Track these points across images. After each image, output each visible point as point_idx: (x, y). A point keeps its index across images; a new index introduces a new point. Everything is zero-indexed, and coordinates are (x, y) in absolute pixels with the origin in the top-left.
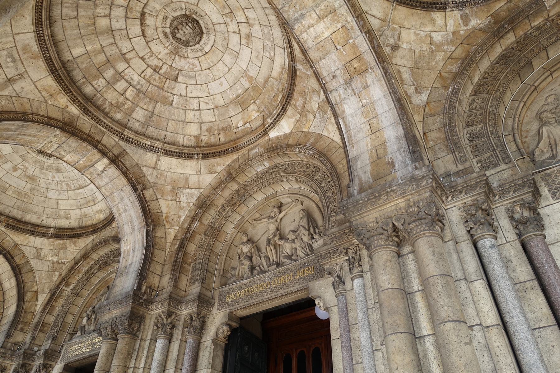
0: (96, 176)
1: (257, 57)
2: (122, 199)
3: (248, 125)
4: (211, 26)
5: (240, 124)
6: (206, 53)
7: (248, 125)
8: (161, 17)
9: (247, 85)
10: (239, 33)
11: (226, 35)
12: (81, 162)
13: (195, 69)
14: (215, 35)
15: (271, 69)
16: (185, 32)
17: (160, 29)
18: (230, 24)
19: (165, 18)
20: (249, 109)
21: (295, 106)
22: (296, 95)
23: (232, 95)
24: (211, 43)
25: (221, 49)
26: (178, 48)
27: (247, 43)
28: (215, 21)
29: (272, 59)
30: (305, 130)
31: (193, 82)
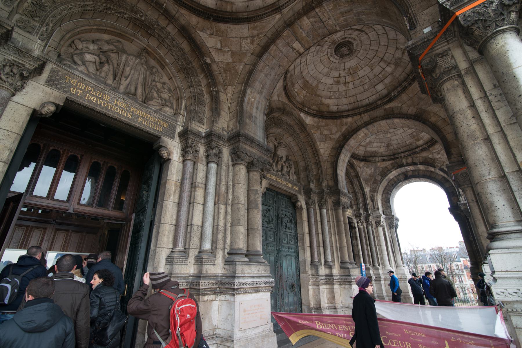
0: (287, 41)
1: (329, 88)
2: (272, 68)
3: (296, 94)
4: (344, 61)
5: (296, 90)
6: (329, 58)
7: (296, 94)
8: (356, 38)
9: (314, 84)
10: (339, 77)
11: (338, 69)
12: (301, 31)
13: (321, 54)
14: (338, 63)
15: (325, 97)
16: (345, 50)
17: (349, 36)
18: (344, 72)
19: (354, 40)
20: (303, 91)
21: (319, 122)
22: (324, 120)
23: (308, 78)
24: (334, 61)
25: (331, 66)
26: (335, 44)
27: (335, 81)
28: (346, 64)
29: (330, 98)
30: (313, 132)
31: (315, 54)
